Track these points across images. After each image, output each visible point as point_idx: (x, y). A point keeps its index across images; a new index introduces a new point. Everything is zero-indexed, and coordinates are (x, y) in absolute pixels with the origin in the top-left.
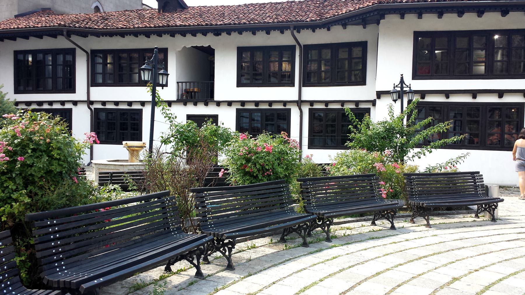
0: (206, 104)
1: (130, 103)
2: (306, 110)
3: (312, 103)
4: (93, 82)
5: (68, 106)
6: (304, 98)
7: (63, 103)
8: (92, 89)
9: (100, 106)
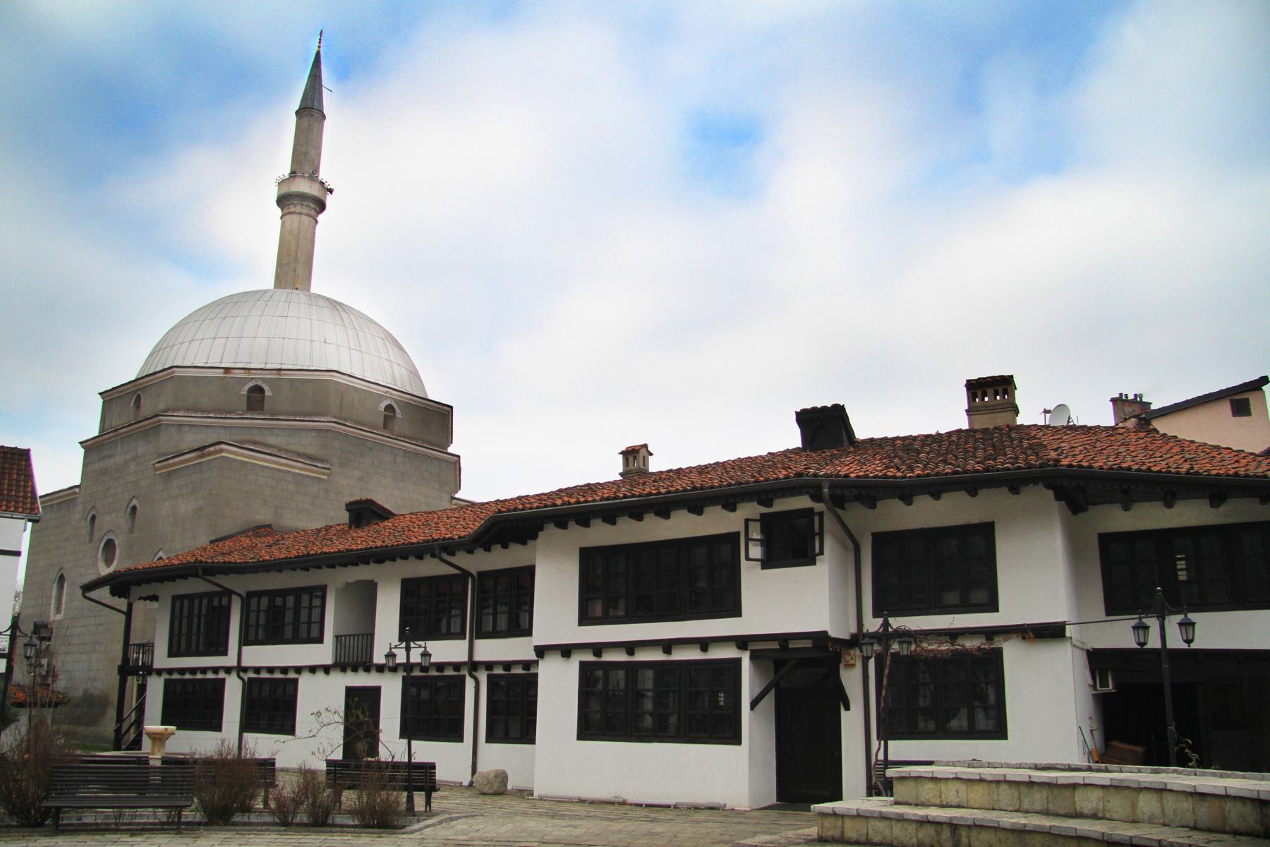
0: (367, 669)
1: (285, 670)
2: (483, 677)
3: (489, 666)
4: (245, 640)
5: (222, 675)
6: (477, 658)
7: (216, 670)
8: (245, 649)
9: (252, 675)
